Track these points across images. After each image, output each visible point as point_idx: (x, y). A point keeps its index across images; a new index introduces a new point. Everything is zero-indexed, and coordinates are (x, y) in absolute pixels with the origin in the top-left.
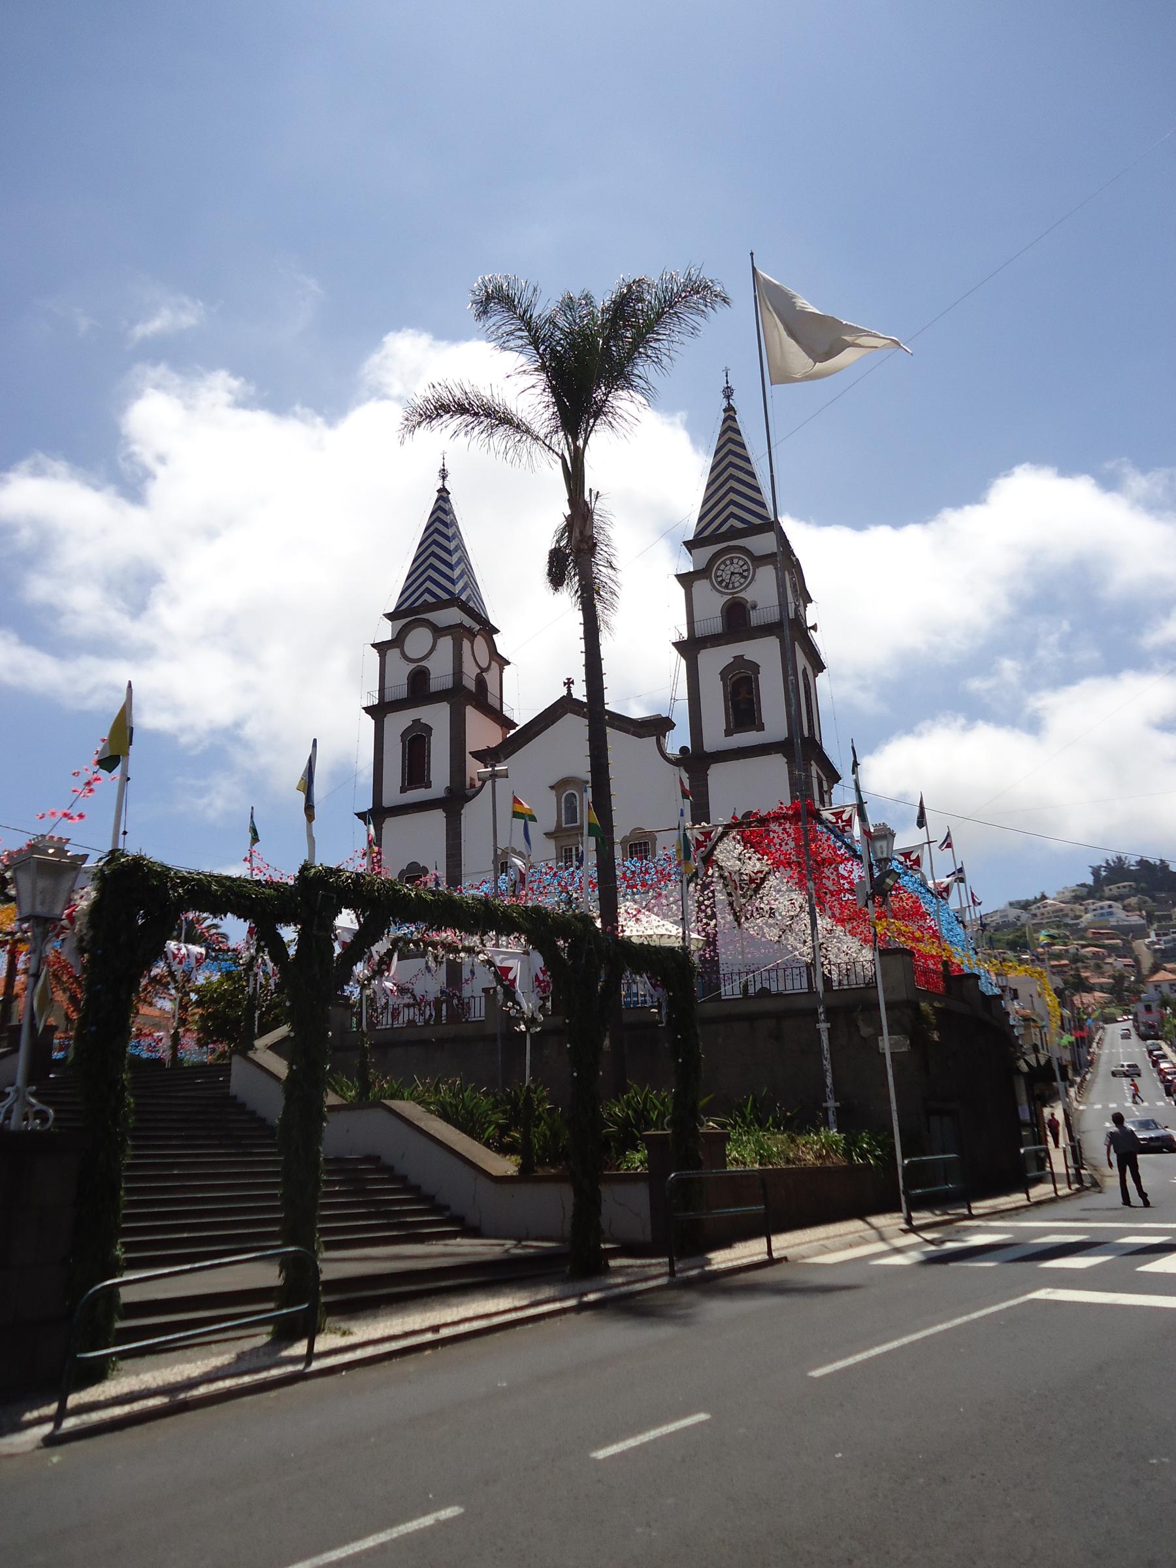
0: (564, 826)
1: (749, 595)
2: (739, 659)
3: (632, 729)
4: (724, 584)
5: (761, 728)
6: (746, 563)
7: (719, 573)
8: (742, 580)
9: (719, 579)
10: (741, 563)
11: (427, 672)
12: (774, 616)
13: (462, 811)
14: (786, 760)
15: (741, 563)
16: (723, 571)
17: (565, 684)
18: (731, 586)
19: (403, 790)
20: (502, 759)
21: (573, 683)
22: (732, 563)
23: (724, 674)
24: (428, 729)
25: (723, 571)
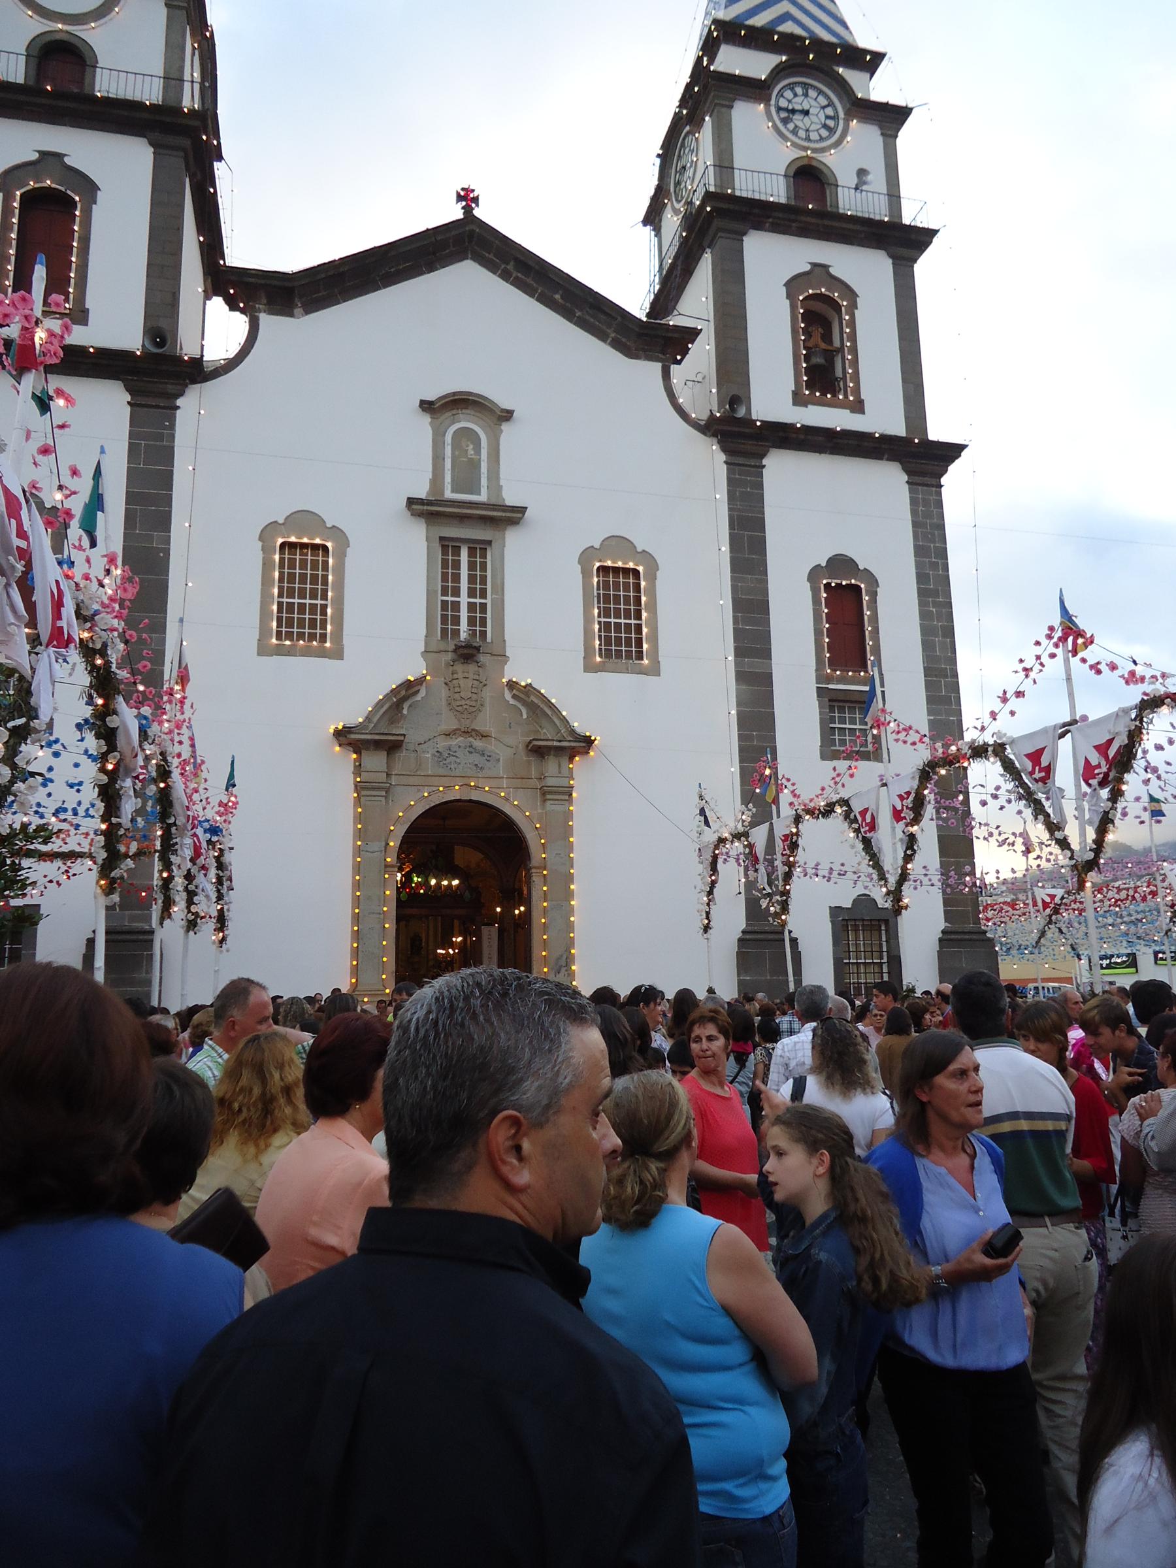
0: (449, 494)
1: (832, 160)
2: (820, 270)
3: (613, 335)
4: (791, 126)
5: (858, 407)
6: (831, 104)
7: (783, 103)
8: (824, 133)
9: (784, 115)
10: (824, 102)
11: (86, 53)
12: (879, 211)
13: (179, 402)
14: (906, 478)
15: (824, 102)
16: (790, 101)
17: (460, 198)
18: (802, 134)
20: (297, 311)
21: (476, 200)
22: (806, 95)
23: (793, 285)
24: (90, 188)
25: (790, 101)
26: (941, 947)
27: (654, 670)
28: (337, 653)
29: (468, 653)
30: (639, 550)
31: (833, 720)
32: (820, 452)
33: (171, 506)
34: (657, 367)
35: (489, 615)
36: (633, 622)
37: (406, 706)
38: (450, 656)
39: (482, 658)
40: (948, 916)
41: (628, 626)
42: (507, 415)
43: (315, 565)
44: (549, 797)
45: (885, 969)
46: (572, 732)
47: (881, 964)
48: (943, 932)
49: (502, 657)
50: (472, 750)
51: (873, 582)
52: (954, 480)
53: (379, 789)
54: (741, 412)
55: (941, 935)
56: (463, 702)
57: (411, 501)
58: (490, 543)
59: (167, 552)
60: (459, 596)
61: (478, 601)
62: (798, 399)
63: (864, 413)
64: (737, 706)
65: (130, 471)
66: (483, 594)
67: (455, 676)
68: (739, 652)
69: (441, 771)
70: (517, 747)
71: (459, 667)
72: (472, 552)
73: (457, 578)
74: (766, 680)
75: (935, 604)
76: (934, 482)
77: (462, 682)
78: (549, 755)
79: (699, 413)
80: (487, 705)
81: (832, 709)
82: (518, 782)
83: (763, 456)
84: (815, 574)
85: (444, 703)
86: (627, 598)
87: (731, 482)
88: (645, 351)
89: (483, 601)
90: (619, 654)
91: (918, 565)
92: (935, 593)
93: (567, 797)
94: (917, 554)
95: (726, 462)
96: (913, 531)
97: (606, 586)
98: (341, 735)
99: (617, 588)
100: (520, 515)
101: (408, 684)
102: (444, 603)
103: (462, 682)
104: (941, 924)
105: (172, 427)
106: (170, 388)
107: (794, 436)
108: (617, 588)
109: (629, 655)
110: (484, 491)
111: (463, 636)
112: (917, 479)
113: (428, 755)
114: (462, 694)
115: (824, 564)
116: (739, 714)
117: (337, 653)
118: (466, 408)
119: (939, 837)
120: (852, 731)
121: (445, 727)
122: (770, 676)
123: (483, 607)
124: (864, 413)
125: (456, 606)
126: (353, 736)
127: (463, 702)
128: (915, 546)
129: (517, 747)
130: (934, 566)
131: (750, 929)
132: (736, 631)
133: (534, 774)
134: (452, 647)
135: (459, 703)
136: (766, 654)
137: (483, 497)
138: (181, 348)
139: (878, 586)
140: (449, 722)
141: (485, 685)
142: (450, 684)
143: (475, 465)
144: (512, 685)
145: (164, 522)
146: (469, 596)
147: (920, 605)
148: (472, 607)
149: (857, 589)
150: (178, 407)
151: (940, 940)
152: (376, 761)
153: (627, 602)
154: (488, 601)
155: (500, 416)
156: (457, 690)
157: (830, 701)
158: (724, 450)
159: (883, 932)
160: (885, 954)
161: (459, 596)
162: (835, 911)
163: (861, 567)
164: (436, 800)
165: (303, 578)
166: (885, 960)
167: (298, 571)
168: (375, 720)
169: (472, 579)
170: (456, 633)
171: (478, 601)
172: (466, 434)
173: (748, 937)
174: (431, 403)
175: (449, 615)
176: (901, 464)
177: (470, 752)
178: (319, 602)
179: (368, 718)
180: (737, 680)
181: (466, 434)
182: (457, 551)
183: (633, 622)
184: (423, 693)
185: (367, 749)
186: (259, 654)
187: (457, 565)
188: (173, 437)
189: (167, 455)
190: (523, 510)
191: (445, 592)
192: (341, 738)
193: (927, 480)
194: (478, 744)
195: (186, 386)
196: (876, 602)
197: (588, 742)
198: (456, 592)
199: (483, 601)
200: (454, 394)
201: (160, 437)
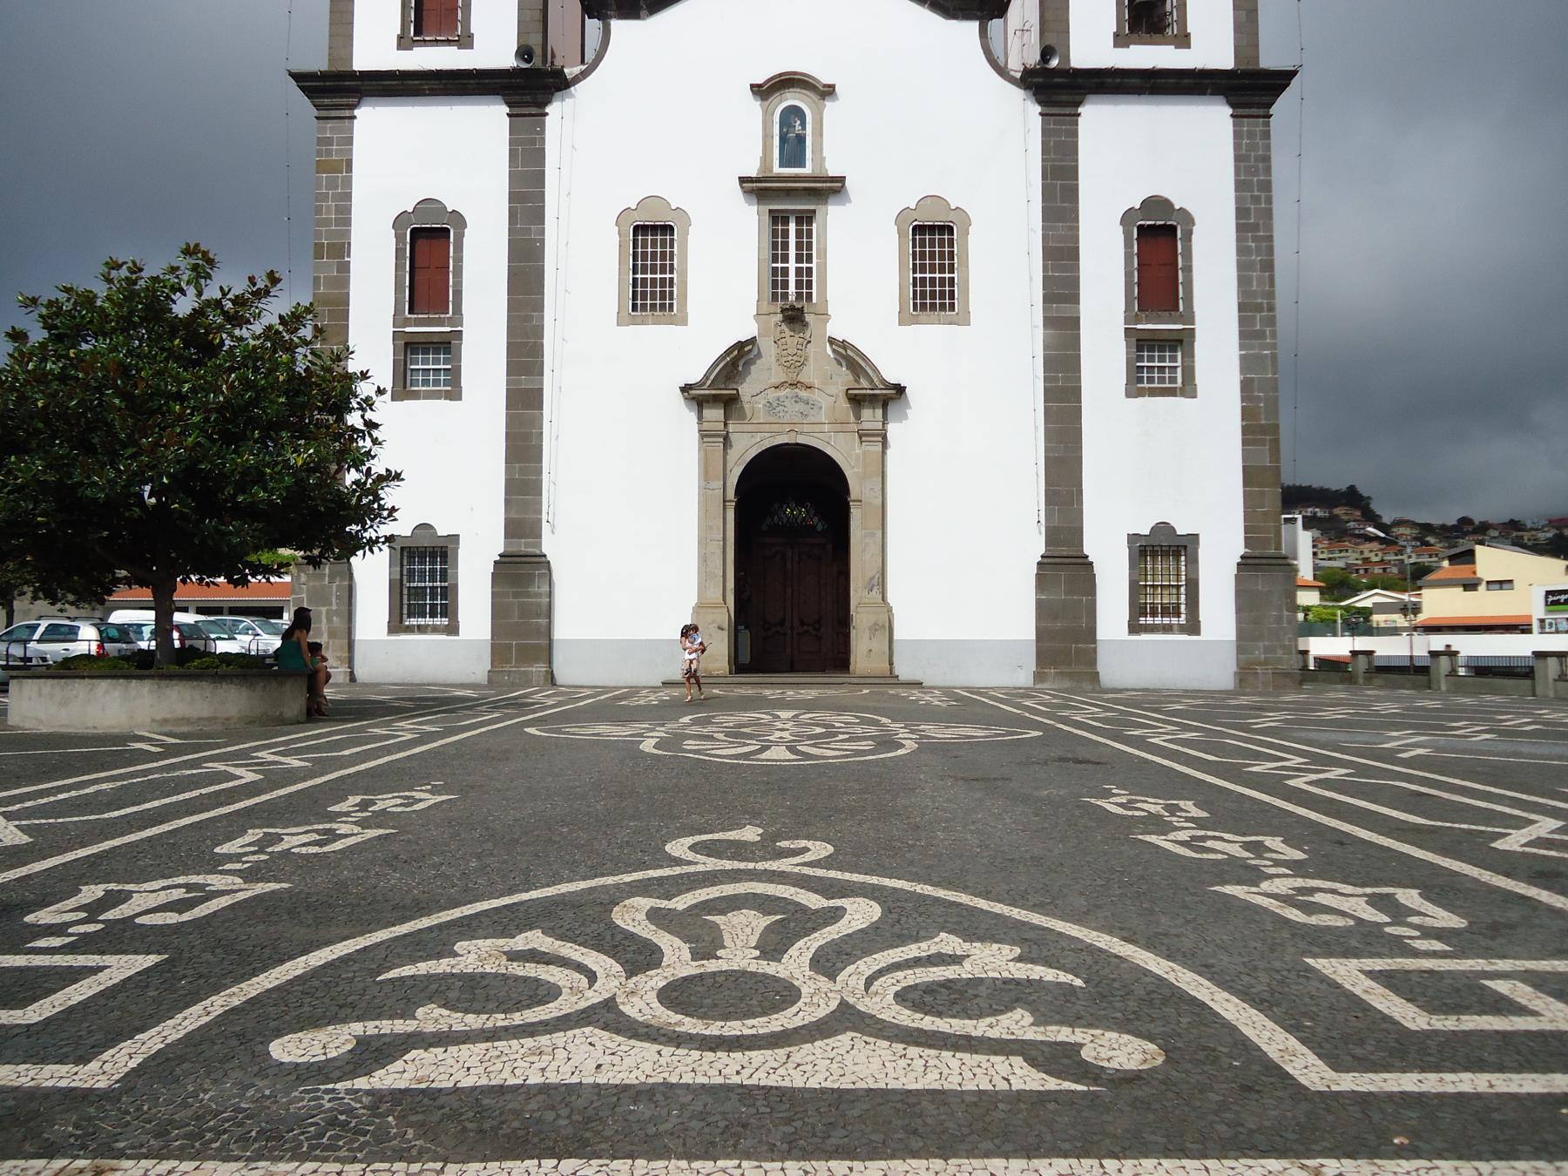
0: (777, 170)
5: (1183, 40)
14: (1230, 111)
19: (404, 43)
20: (643, 13)
26: (1238, 570)
27: (965, 320)
28: (683, 321)
29: (794, 317)
30: (953, 207)
31: (1140, 359)
32: (1139, 94)
33: (544, 202)
34: (974, 26)
35: (814, 278)
36: (947, 275)
37: (741, 363)
38: (780, 317)
39: (808, 318)
40: (1248, 542)
41: (942, 280)
42: (828, 92)
43: (663, 245)
44: (863, 439)
45: (1183, 590)
46: (883, 381)
47: (1178, 587)
48: (1242, 557)
49: (824, 315)
50: (798, 399)
51: (1187, 218)
52: (1283, 107)
53: (719, 436)
54: (1054, 63)
55: (1240, 560)
56: (790, 358)
57: (742, 180)
58: (814, 211)
59: (542, 241)
60: (788, 262)
61: (805, 265)
62: (1120, 40)
63: (1189, 47)
64: (1045, 349)
65: (513, 176)
66: (809, 260)
67: (783, 335)
68: (1048, 299)
69: (772, 419)
70: (837, 396)
71: (783, 325)
72: (799, 221)
73: (785, 246)
74: (1075, 323)
75: (1255, 239)
76: (1261, 112)
77: (789, 340)
78: (865, 401)
79: (1015, 66)
80: (811, 359)
81: (1140, 348)
82: (839, 427)
83: (1079, 104)
84: (1127, 217)
85: (773, 359)
86: (942, 254)
87: (1045, 132)
88: (961, 9)
89: (808, 265)
90: (933, 307)
91: (1238, 200)
92: (1255, 227)
93: (880, 439)
94: (1236, 190)
95: (1041, 114)
96: (1236, 166)
97: (923, 245)
98: (686, 389)
99: (932, 244)
100: (840, 185)
101: (740, 346)
102: (775, 270)
103: (789, 340)
104: (1241, 549)
105: (543, 132)
106: (540, 98)
107: (1110, 80)
108: (932, 244)
109: (943, 307)
110: (809, 163)
111: (792, 298)
112: (1241, 111)
113: (761, 406)
114: (789, 351)
115: (1138, 207)
116: (1045, 357)
117: (683, 321)
118: (793, 87)
119: (1244, 468)
120: (1161, 369)
121: (775, 380)
122: (1079, 318)
123: (809, 270)
124: (1189, 47)
125: (785, 271)
126: (693, 392)
127: (790, 358)
128: (1236, 180)
129: (837, 396)
130: (1256, 200)
131: (1049, 554)
132: (1045, 278)
133: (852, 419)
134: (779, 311)
135: (785, 359)
136: (1075, 299)
137: (807, 170)
138: (553, 56)
139: (1194, 225)
140: (779, 376)
141: (810, 342)
142: (779, 343)
143: (801, 139)
144: (832, 341)
145: (538, 216)
146: (796, 262)
147: (1239, 240)
148: (799, 271)
149: (1173, 229)
150: (547, 114)
151: (1238, 564)
152: (715, 414)
153: (942, 257)
154: (814, 265)
155: (824, 92)
156: (784, 347)
157: (1138, 340)
158: (1040, 102)
159: (1183, 558)
160: (1183, 578)
161: (788, 262)
162: (1133, 538)
163: (1177, 207)
164: (767, 444)
165: (654, 254)
166: (1184, 583)
167: (649, 250)
168: (712, 377)
169: (799, 246)
170: (785, 296)
171: (805, 265)
172: (793, 113)
173: (1046, 560)
174: (759, 86)
175: (777, 280)
176: (1226, 97)
177: (796, 402)
178: (668, 276)
179: (706, 376)
180: (1045, 326)
181: (793, 113)
182: (786, 222)
183: (947, 275)
184: (755, 352)
185: (708, 402)
186: (618, 325)
187: (786, 234)
188: (544, 139)
189: (538, 156)
190: (842, 179)
191: (775, 260)
192: (686, 394)
193: (1254, 111)
194: (804, 394)
195: (553, 94)
196: (1190, 240)
197: (900, 390)
198: (785, 259)
199: (808, 265)
200: (780, 75)
201: (533, 141)
